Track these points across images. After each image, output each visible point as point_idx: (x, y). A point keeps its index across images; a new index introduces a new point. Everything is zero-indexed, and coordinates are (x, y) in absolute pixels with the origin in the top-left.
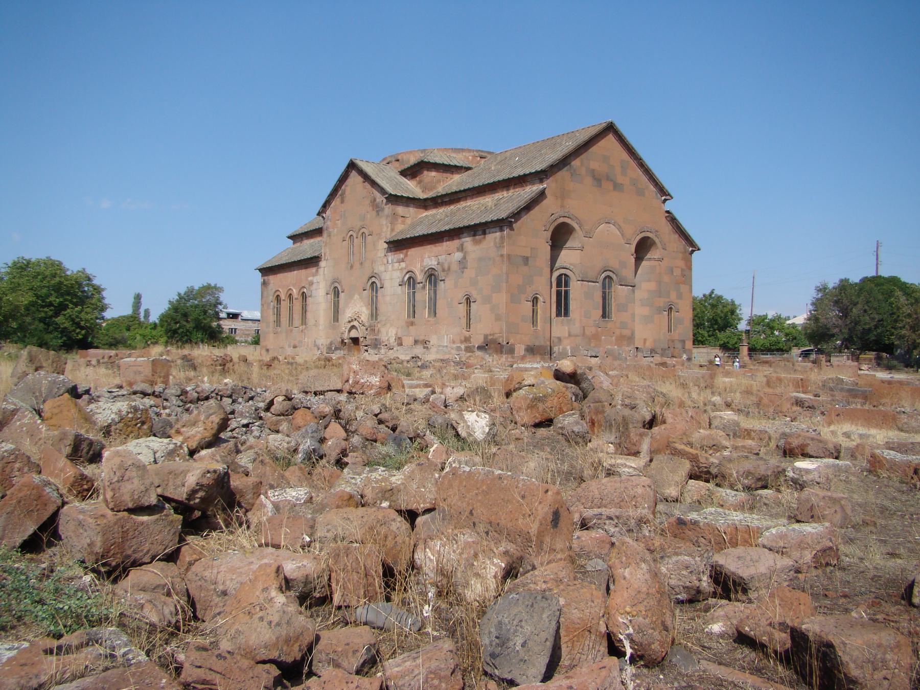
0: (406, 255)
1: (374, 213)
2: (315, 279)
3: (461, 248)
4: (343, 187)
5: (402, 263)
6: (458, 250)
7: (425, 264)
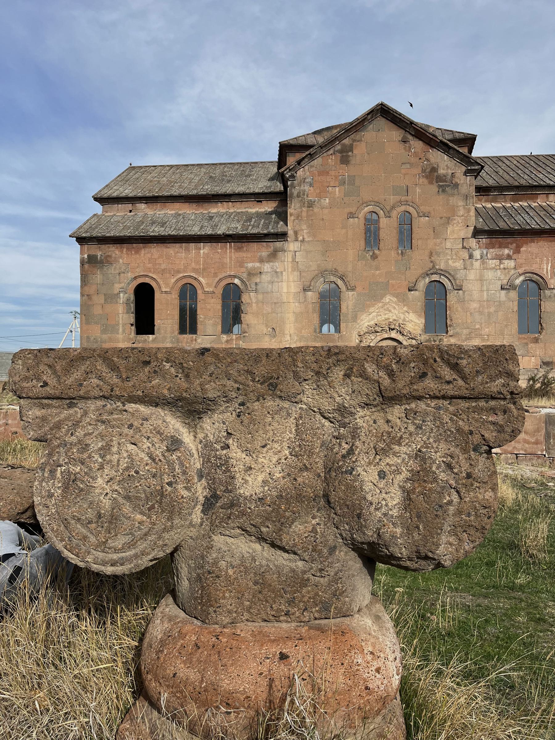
0: (517, 251)
1: (434, 188)
2: (267, 267)
4: (346, 141)
5: (506, 262)
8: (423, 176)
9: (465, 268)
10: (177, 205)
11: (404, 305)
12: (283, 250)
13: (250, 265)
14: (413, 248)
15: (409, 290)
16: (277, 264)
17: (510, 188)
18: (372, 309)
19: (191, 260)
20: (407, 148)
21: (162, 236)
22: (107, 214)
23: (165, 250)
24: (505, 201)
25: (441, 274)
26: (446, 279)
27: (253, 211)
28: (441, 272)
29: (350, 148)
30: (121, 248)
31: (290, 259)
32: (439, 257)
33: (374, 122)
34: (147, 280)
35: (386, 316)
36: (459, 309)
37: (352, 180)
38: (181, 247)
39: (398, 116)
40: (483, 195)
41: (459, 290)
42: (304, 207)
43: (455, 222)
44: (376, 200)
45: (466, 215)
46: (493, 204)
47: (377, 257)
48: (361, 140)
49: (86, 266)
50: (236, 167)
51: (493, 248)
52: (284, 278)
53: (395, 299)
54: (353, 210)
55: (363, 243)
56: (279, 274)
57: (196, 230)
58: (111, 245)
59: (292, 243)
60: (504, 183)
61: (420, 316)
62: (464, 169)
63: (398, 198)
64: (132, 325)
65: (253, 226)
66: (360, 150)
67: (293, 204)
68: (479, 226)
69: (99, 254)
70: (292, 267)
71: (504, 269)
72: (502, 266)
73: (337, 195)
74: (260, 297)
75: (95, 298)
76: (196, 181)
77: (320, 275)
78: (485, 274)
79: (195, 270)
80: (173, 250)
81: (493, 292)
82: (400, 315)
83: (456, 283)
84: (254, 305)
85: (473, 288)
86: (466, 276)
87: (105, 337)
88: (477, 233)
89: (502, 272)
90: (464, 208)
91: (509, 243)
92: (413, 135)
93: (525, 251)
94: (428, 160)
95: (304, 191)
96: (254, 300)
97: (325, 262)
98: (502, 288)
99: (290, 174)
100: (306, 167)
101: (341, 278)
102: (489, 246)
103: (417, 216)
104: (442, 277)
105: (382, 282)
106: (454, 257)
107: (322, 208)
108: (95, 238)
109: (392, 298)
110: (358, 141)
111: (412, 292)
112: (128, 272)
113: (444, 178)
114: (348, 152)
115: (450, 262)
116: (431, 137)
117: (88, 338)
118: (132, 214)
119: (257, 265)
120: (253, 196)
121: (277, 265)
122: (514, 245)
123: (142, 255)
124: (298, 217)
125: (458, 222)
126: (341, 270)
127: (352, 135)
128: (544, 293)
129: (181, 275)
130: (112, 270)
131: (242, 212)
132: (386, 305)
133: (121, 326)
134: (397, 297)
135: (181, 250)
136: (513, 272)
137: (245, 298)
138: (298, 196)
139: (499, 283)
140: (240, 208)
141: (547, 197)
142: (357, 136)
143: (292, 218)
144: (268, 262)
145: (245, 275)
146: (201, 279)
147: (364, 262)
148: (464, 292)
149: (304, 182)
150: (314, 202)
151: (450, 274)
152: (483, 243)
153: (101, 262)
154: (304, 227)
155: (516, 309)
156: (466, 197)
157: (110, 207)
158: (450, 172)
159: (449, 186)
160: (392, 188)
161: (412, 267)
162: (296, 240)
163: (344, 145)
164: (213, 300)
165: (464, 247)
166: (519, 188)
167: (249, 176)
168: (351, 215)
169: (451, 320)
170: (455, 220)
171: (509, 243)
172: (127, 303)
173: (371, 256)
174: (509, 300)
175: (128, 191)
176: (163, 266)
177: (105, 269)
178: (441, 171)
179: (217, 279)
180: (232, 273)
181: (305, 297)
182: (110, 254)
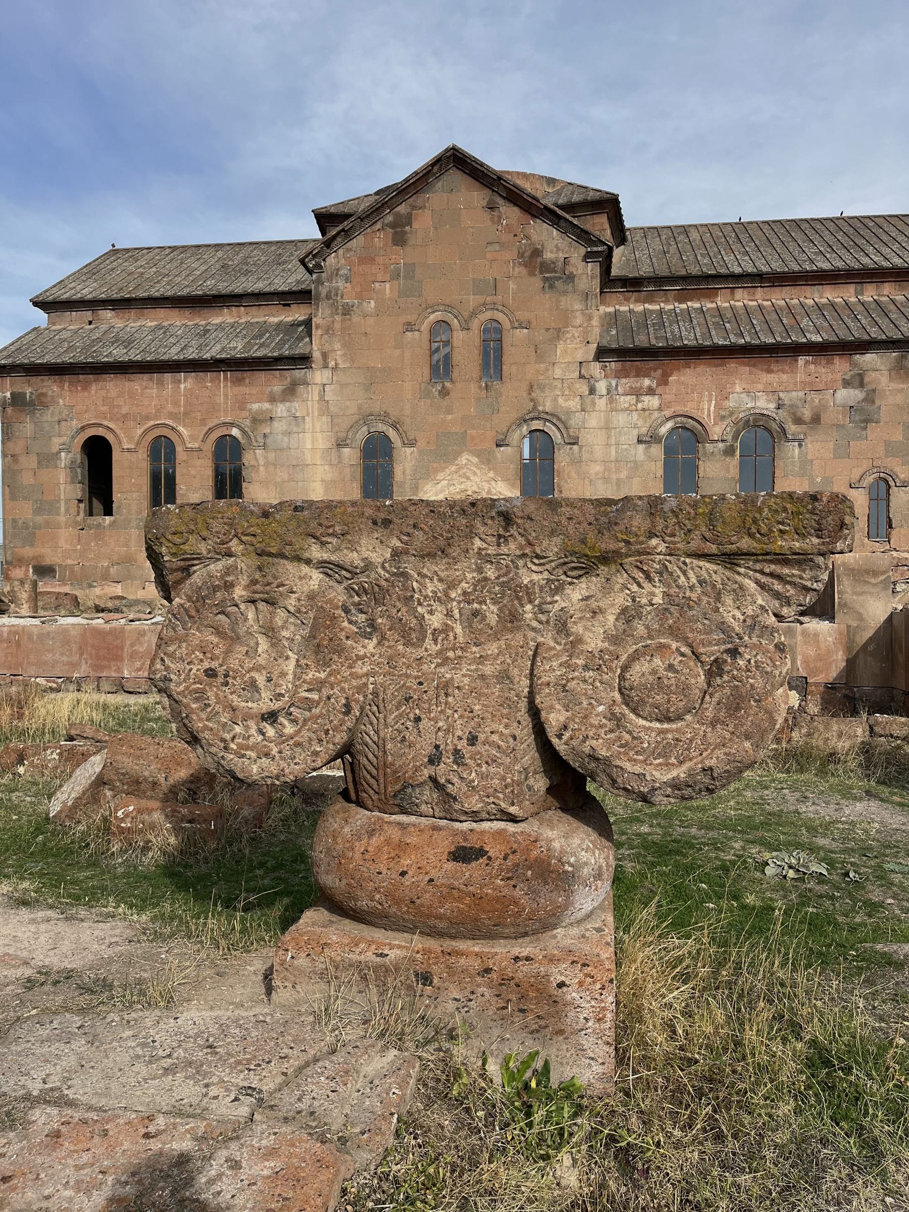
0: (664, 381)
1: (536, 282)
2: (281, 409)
3: (858, 380)
4: (402, 209)
5: (646, 399)
6: (846, 384)
7: (731, 403)
8: (520, 264)
9: (583, 410)
10: (161, 313)
11: (490, 470)
12: (306, 383)
13: (255, 406)
14: (504, 378)
15: (498, 445)
16: (296, 404)
17: (673, 279)
18: (440, 476)
19: (167, 400)
20: (496, 219)
21: (119, 362)
22: (54, 328)
23: (127, 384)
24: (667, 301)
25: (546, 420)
26: (553, 428)
27: (275, 320)
28: (546, 416)
29: (408, 220)
30: (61, 382)
31: (316, 397)
32: (544, 392)
33: (445, 177)
34: (100, 432)
35: (463, 487)
36: (573, 474)
37: (410, 270)
38: (151, 379)
39: (479, 167)
40: (632, 292)
41: (573, 444)
42: (337, 314)
43: (568, 336)
44: (447, 302)
45: (585, 325)
46: (647, 305)
47: (449, 394)
48: (425, 207)
49: (9, 410)
50: (273, 248)
51: (627, 376)
52: (307, 426)
53: (475, 460)
54: (411, 318)
55: (426, 371)
56: (300, 420)
57: (173, 354)
58: (47, 377)
59: (319, 372)
60: (664, 272)
61: (513, 485)
62: (583, 251)
63: (481, 299)
64: (80, 501)
65: (262, 345)
66: (423, 223)
67: (320, 310)
68: (604, 343)
69: (28, 391)
70: (320, 409)
71: (644, 410)
72: (640, 406)
73: (388, 296)
74: (271, 456)
75: (23, 459)
76: (199, 273)
77: (361, 422)
78: (614, 418)
79: (172, 416)
80: (139, 384)
81: (625, 447)
82: (483, 483)
83: (568, 434)
84: (261, 468)
85: (595, 442)
86: (583, 422)
87: (39, 519)
88: (602, 353)
89: (639, 415)
90: (582, 313)
91: (651, 369)
92: (504, 198)
93: (677, 382)
94: (527, 237)
95: (337, 289)
96: (262, 462)
97: (369, 401)
98: (640, 441)
99: (314, 262)
100: (341, 252)
101: (394, 426)
102: (619, 375)
103: (509, 327)
104: (547, 424)
105: (456, 433)
106: (567, 393)
107: (364, 317)
108: (19, 366)
109: (470, 458)
110: (420, 208)
111: (502, 449)
112: (72, 419)
113: (552, 265)
114: (404, 226)
115: (561, 400)
116: (530, 200)
117: (14, 521)
118: (92, 326)
119: (267, 406)
120: (276, 298)
121: (297, 407)
122: (660, 371)
123: (93, 392)
124: (328, 330)
125: (573, 336)
126: (394, 413)
127: (411, 199)
128: (704, 447)
129: (152, 423)
130: (48, 417)
131: (257, 322)
132: (463, 468)
133: (62, 502)
134: (478, 456)
135: (151, 384)
136: (656, 415)
137: (248, 458)
138: (328, 297)
139: (635, 433)
140: (257, 316)
141: (733, 294)
142: (418, 200)
143: (320, 332)
144: (283, 401)
145: (248, 422)
146: (181, 429)
147: (429, 401)
148: (581, 447)
149: (337, 275)
150: (352, 306)
151: (559, 419)
152: (611, 369)
153: (32, 404)
154: (337, 346)
155: (660, 472)
156: (586, 296)
157: (58, 316)
158: (561, 256)
159: (560, 278)
160: (471, 282)
161: (501, 410)
162: (326, 367)
163: (398, 215)
164: (199, 462)
165: (581, 377)
166: (687, 279)
167: (285, 262)
168: (409, 327)
169: (561, 492)
170: (568, 332)
171: (651, 369)
172: (71, 467)
173: (440, 392)
174: (650, 458)
175: (87, 291)
176: (125, 410)
177: (38, 415)
178: (548, 255)
179: (206, 429)
180: (228, 419)
181: (340, 457)
182: (44, 390)
